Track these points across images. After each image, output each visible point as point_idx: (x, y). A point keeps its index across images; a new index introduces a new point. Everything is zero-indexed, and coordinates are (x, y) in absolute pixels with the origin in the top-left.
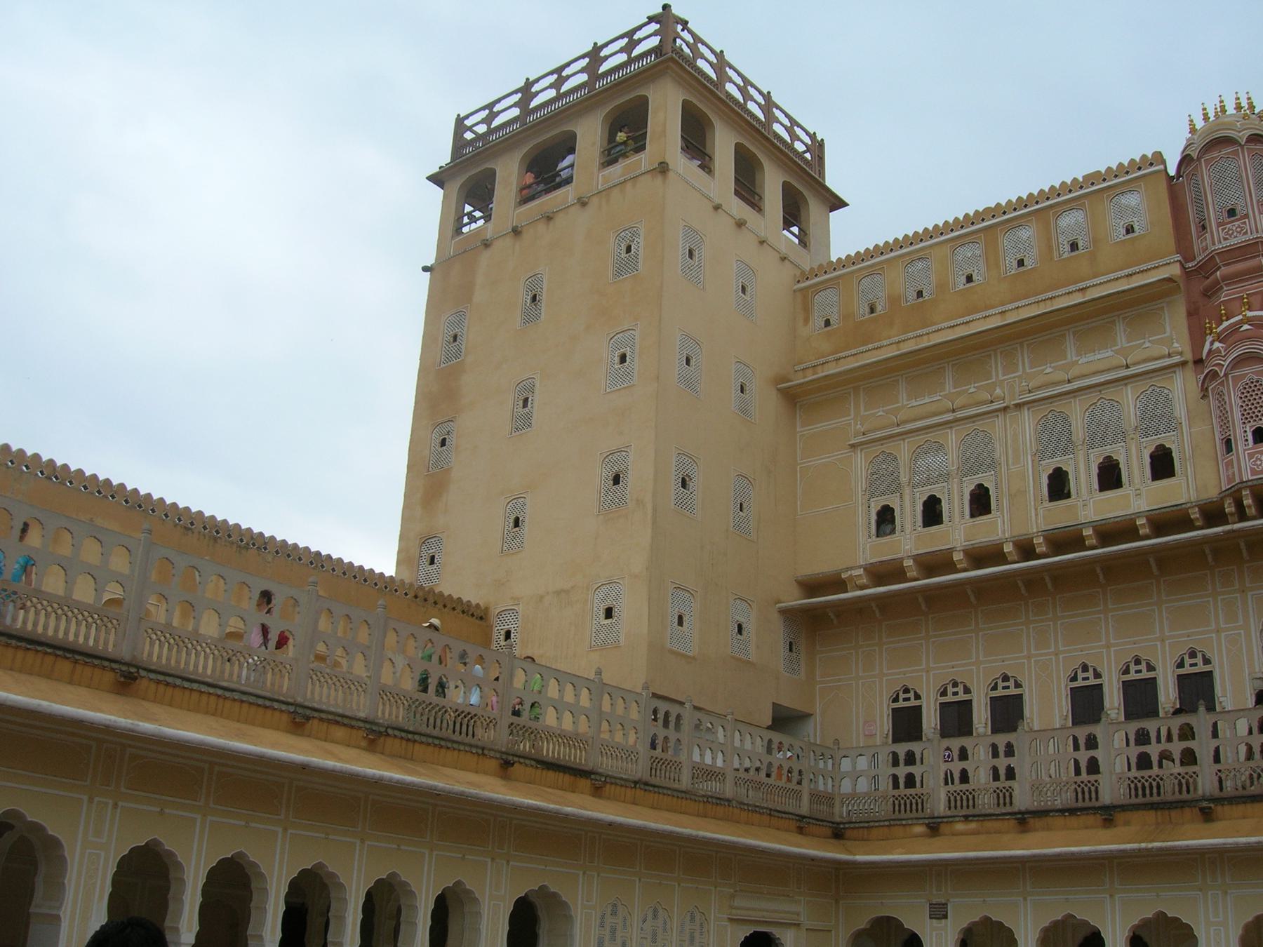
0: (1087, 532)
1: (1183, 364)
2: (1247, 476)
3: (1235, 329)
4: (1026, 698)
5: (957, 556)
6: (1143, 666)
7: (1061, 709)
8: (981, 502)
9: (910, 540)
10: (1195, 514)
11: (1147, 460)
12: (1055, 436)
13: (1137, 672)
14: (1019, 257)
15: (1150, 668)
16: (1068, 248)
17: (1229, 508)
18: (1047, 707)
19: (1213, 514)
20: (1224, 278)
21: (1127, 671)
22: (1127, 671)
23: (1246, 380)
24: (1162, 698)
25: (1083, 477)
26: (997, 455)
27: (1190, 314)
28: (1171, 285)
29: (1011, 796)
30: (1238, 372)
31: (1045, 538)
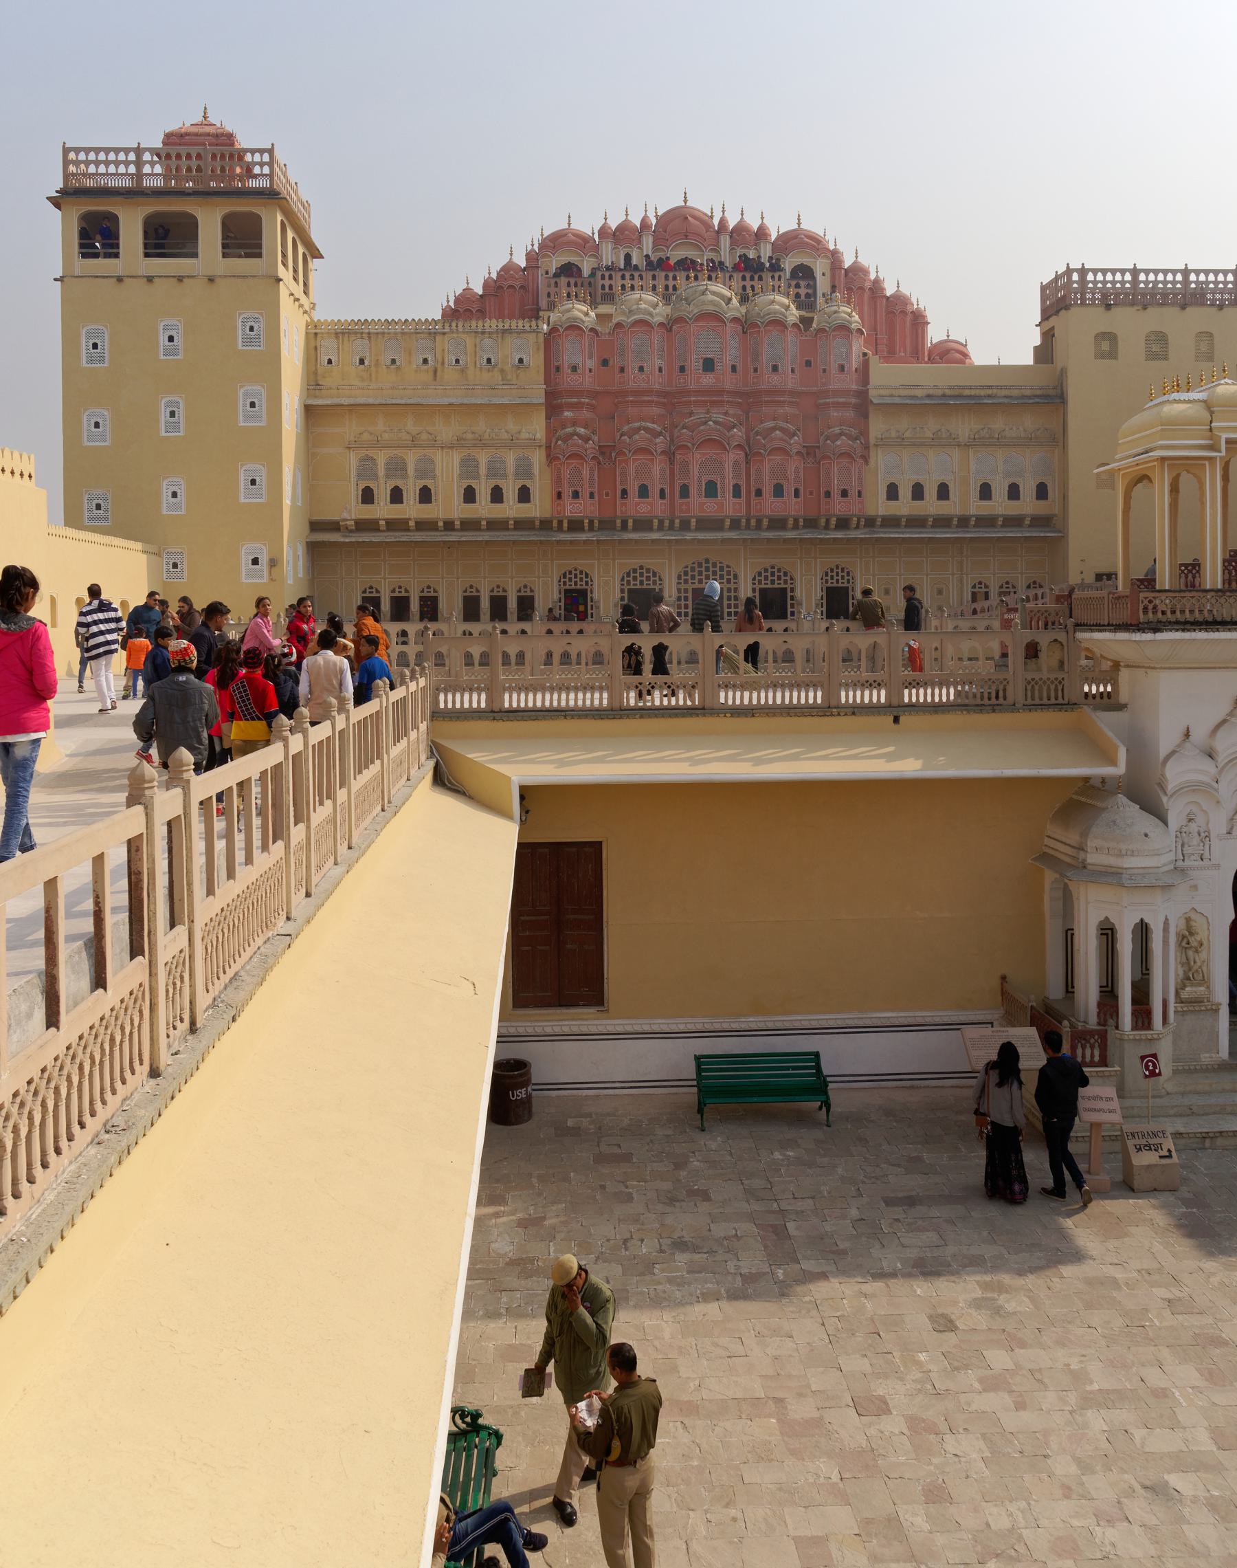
2: (568, 514)
4: (440, 599)
7: (459, 604)
8: (425, 495)
9: (383, 509)
10: (537, 523)
12: (469, 467)
17: (555, 524)
19: (545, 525)
22: (492, 591)
24: (509, 606)
25: (483, 493)
26: (438, 472)
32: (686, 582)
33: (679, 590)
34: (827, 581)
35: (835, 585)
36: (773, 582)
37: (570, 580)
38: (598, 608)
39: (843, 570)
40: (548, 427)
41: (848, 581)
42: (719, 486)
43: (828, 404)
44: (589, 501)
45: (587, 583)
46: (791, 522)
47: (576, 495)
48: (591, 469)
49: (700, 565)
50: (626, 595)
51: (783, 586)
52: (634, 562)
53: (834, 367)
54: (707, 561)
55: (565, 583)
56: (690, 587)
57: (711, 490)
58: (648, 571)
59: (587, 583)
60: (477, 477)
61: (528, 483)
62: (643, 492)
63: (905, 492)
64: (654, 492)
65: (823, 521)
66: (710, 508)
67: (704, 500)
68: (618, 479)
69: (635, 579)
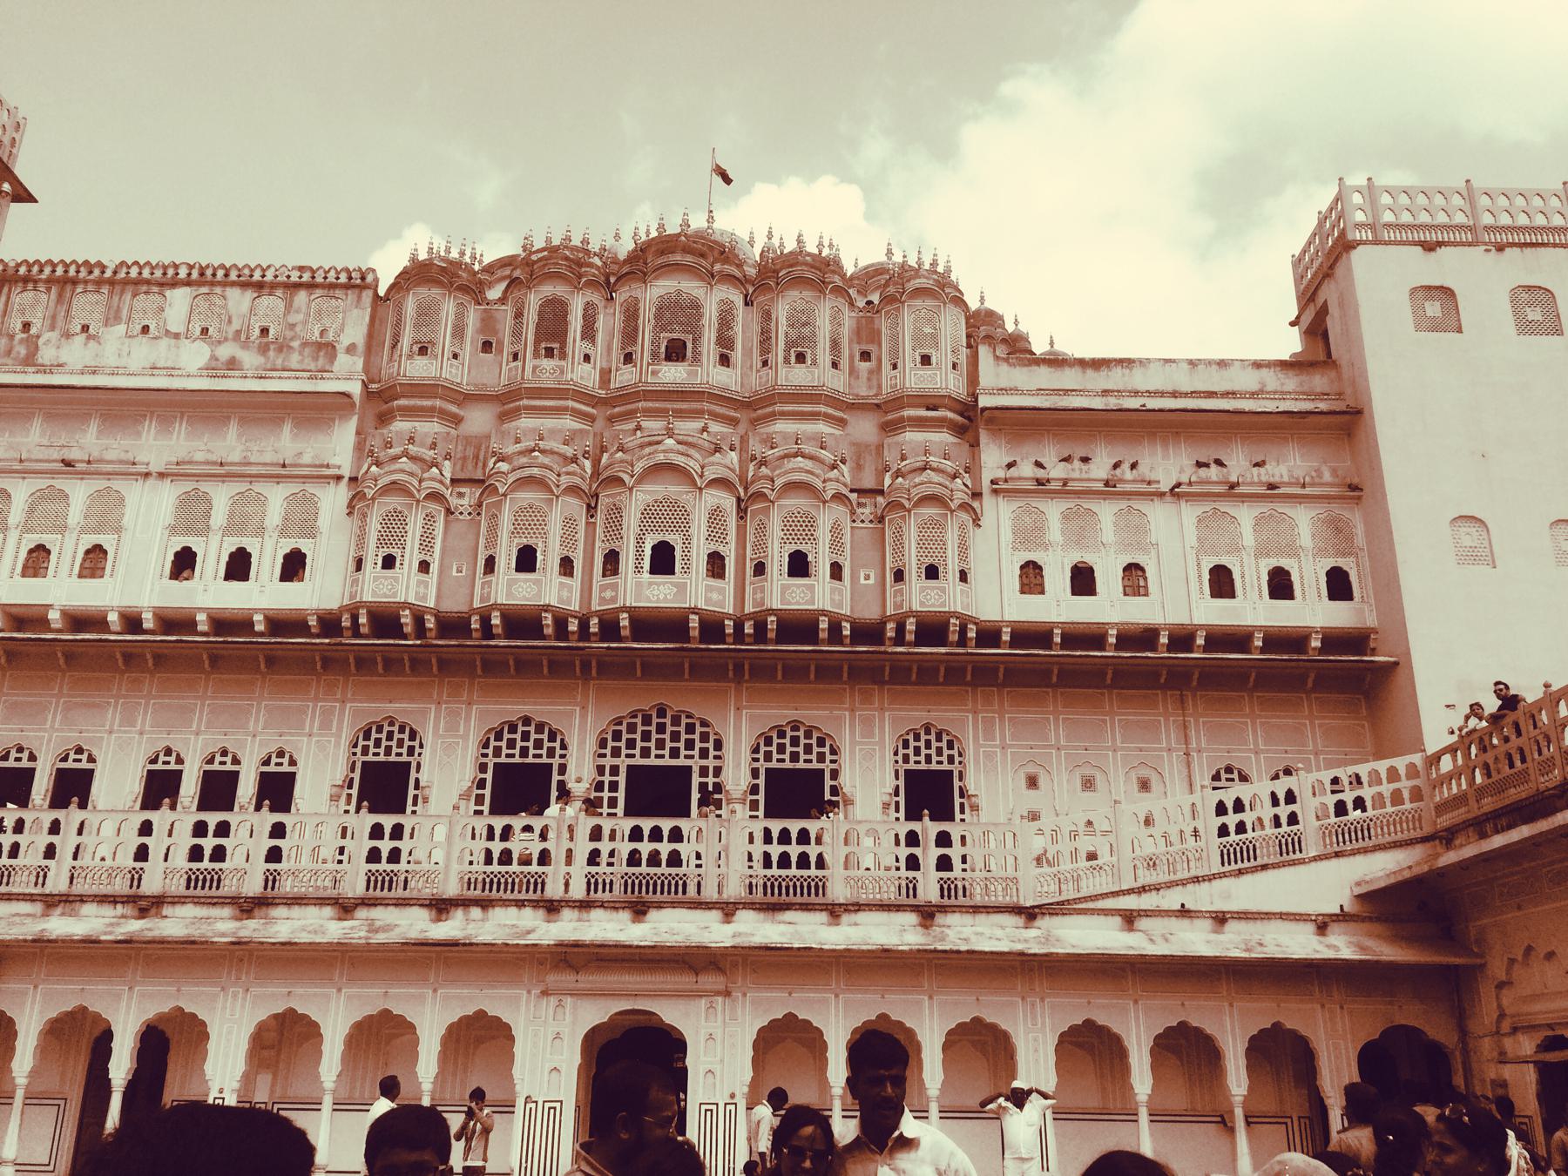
0: (201, 617)
1: (339, 478)
3: (396, 458)
5: (54, 615)
6: (228, 759)
7: (134, 786)
8: (94, 561)
10: (313, 622)
11: (280, 561)
12: (192, 514)
13: (223, 763)
14: (204, 324)
15: (236, 761)
16: (257, 332)
17: (346, 623)
18: (117, 785)
19: (330, 623)
20: (401, 409)
21: (211, 761)
22: (211, 761)
23: (391, 508)
25: (212, 559)
26: (125, 521)
27: (358, 433)
28: (347, 400)
29: (45, 876)
30: (387, 499)
31: (155, 614)
32: (616, 752)
33: (601, 770)
34: (906, 759)
35: (923, 766)
36: (795, 757)
37: (378, 743)
38: (426, 800)
39: (939, 739)
40: (359, 447)
41: (951, 759)
42: (678, 554)
43: (902, 419)
44: (416, 577)
45: (411, 751)
46: (824, 624)
47: (389, 562)
48: (429, 517)
49: (647, 720)
50: (489, 776)
51: (815, 765)
52: (513, 709)
53: (910, 356)
54: (662, 713)
55: (365, 751)
56: (623, 763)
57: (663, 560)
58: (540, 728)
59: (411, 751)
60: (205, 531)
61: (305, 546)
62: (526, 560)
63: (1057, 579)
64: (549, 558)
65: (891, 626)
66: (658, 594)
67: (646, 575)
68: (482, 541)
69: (511, 744)
